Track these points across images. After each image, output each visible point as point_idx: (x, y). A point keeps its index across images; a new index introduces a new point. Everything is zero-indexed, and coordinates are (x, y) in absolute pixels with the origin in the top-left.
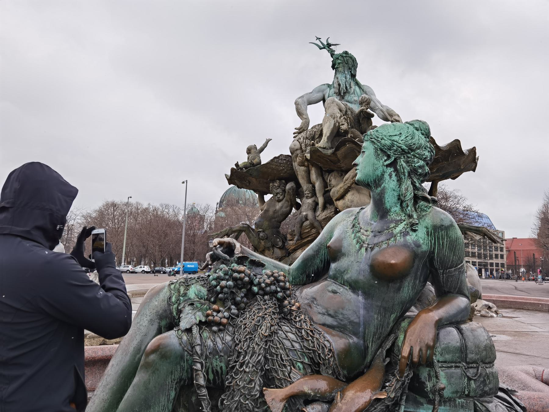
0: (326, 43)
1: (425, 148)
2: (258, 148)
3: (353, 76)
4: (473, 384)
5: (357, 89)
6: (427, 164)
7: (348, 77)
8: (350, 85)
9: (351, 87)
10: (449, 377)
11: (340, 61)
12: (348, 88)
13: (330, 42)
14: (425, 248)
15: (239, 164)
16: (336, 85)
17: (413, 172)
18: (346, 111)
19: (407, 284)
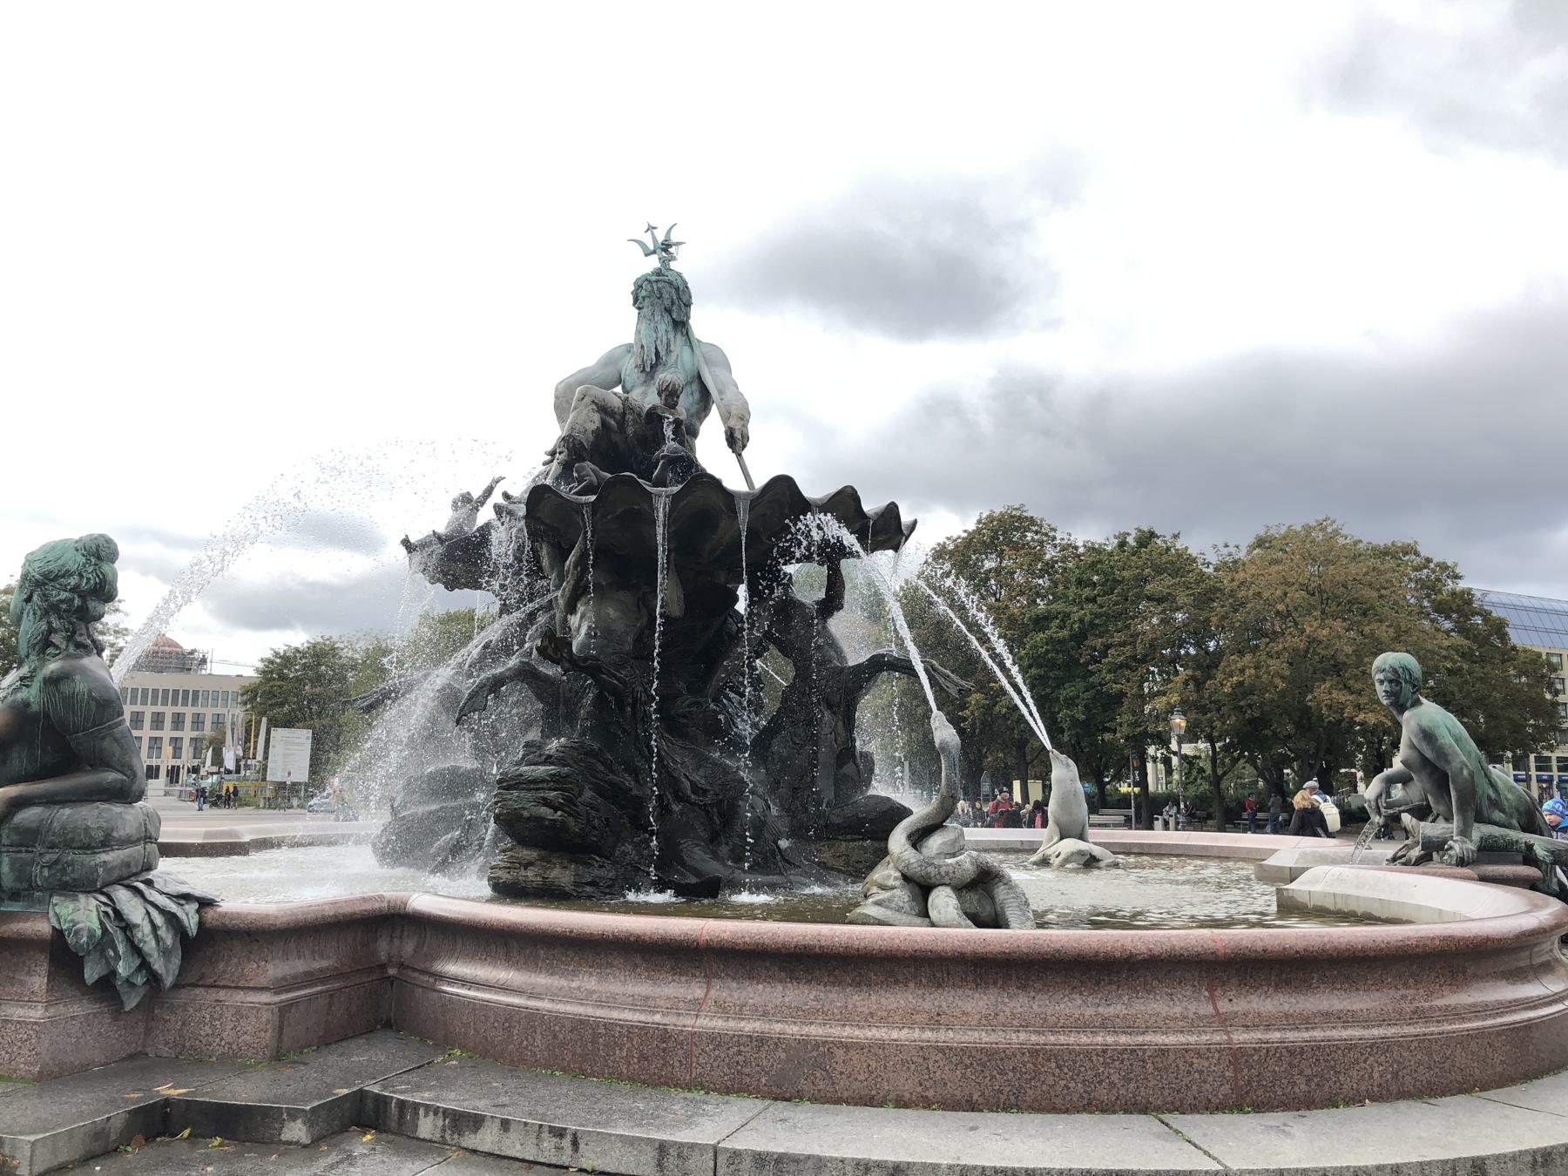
0: (660, 239)
1: (81, 575)
2: (476, 494)
3: (681, 326)
4: (46, 873)
5: (687, 350)
6: (83, 596)
7: (662, 327)
8: (668, 345)
9: (669, 351)
10: (12, 864)
11: (643, 293)
12: (662, 353)
13: (674, 239)
14: (35, 708)
15: (412, 540)
16: (636, 349)
17: (51, 609)
18: (624, 414)
19: (15, 755)
